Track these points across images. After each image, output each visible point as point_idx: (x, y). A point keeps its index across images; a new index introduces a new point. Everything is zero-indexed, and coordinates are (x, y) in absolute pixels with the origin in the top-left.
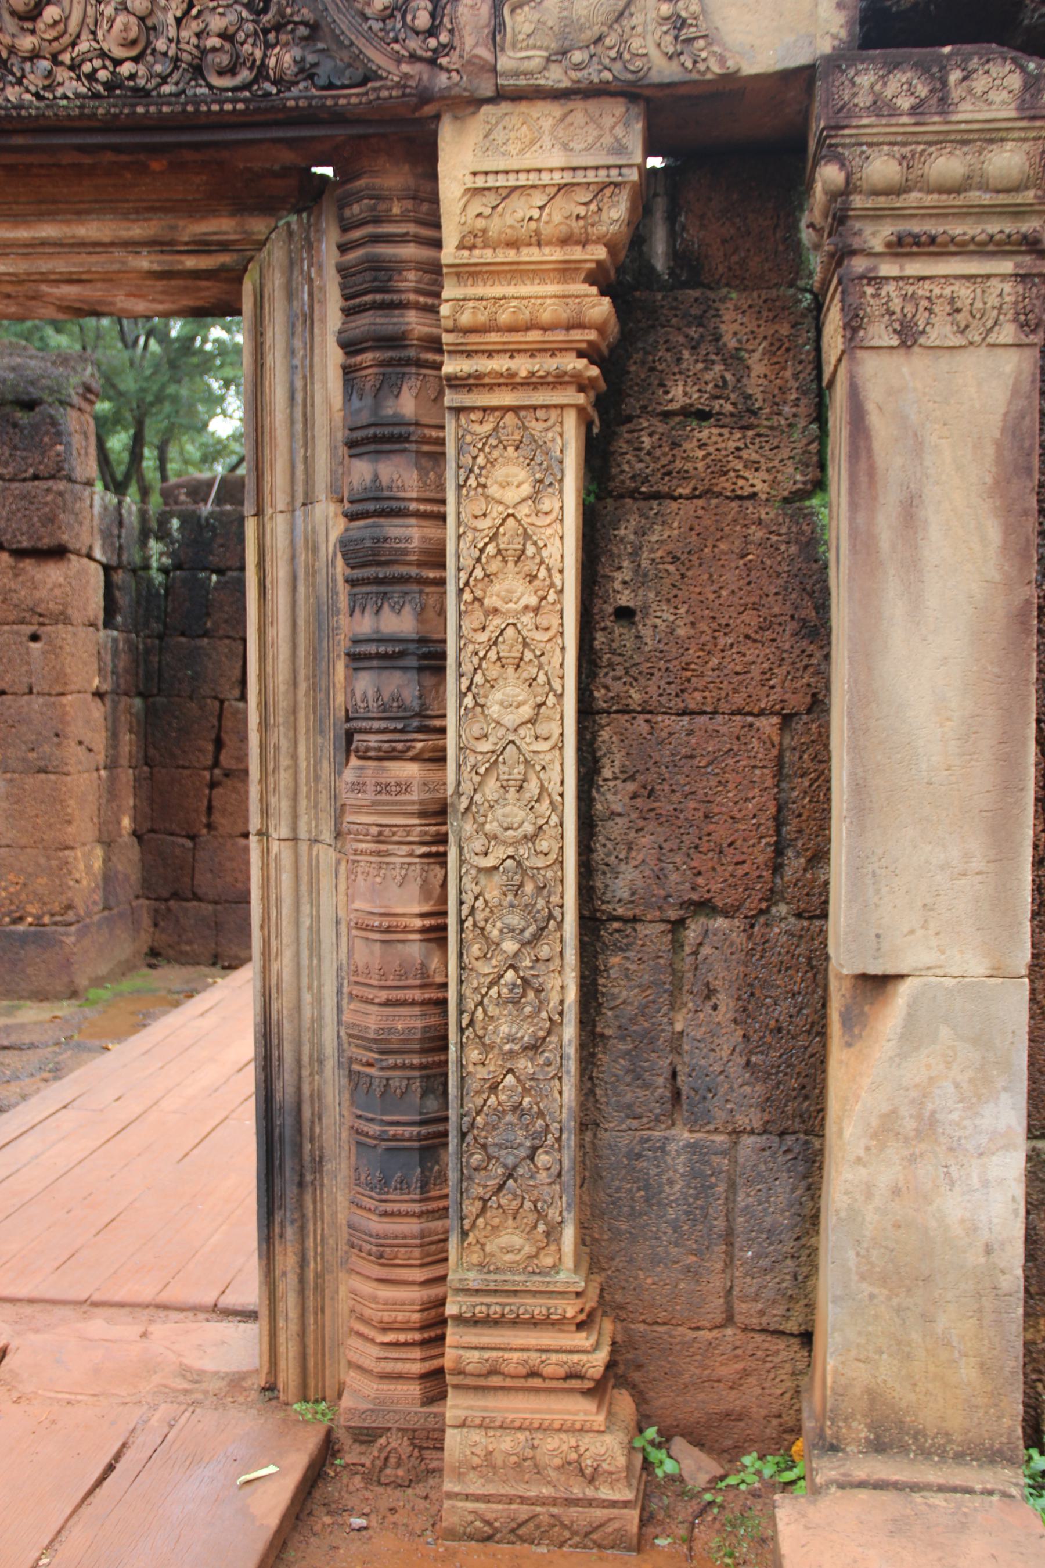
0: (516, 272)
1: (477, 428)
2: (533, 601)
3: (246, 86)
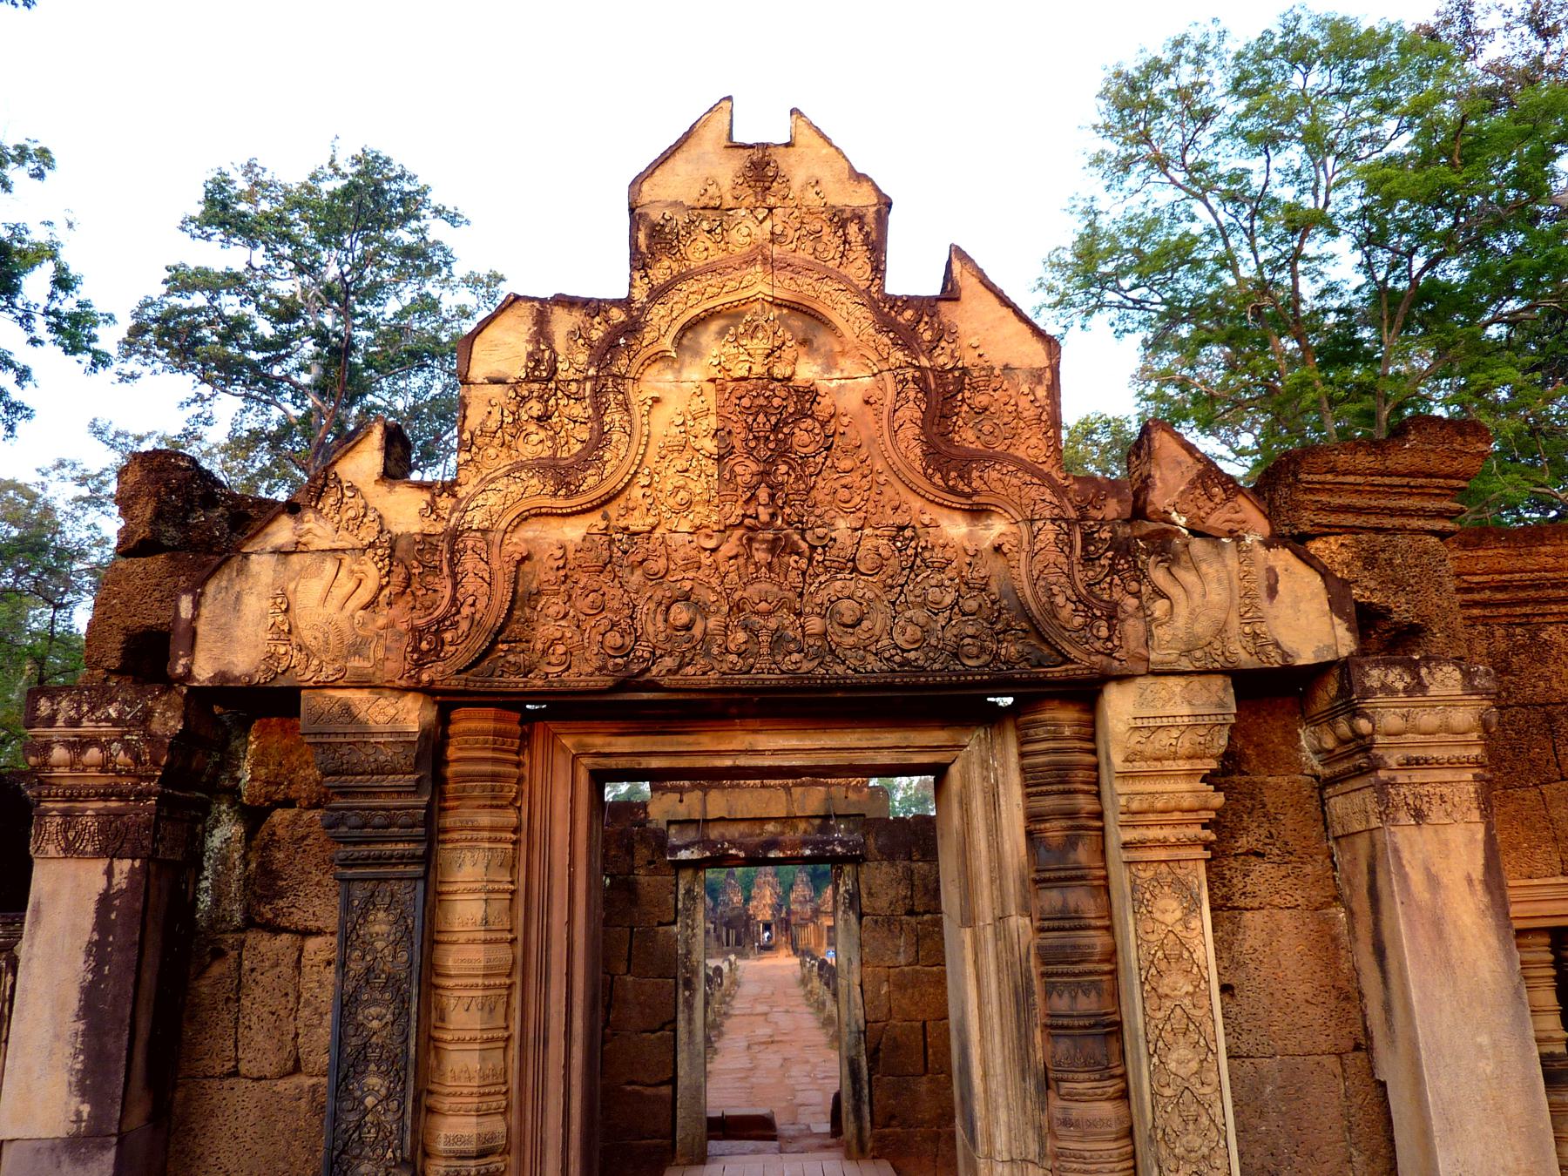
0: (1162, 775)
1: (1142, 874)
2: (1191, 989)
3: (987, 665)
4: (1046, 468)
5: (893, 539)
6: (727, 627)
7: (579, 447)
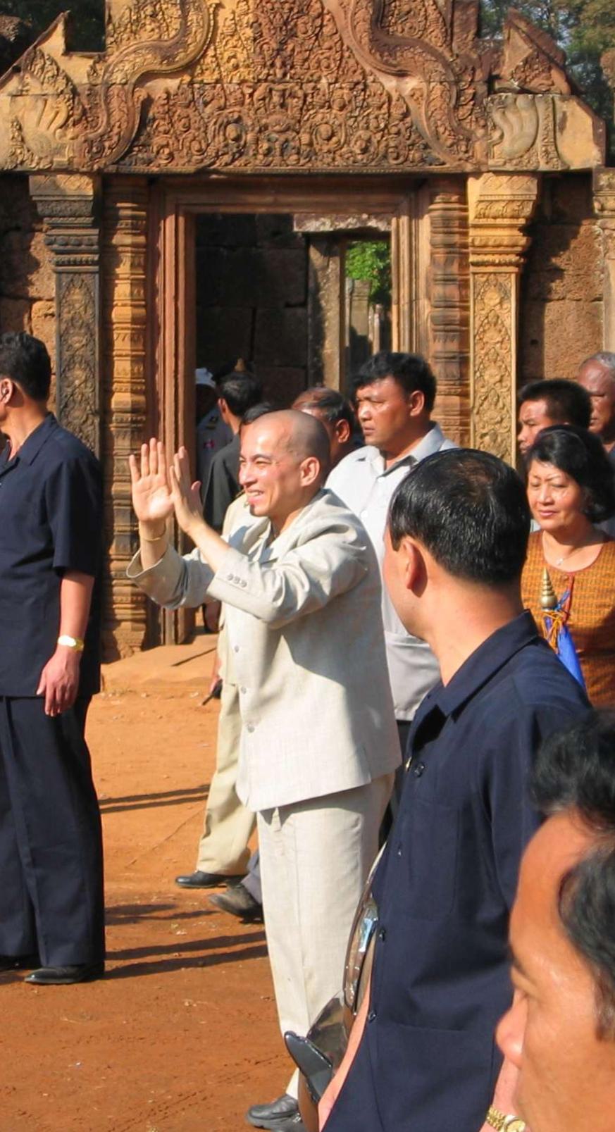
4: (441, 50)
5: (351, 89)
6: (258, 140)
7: (173, 33)
